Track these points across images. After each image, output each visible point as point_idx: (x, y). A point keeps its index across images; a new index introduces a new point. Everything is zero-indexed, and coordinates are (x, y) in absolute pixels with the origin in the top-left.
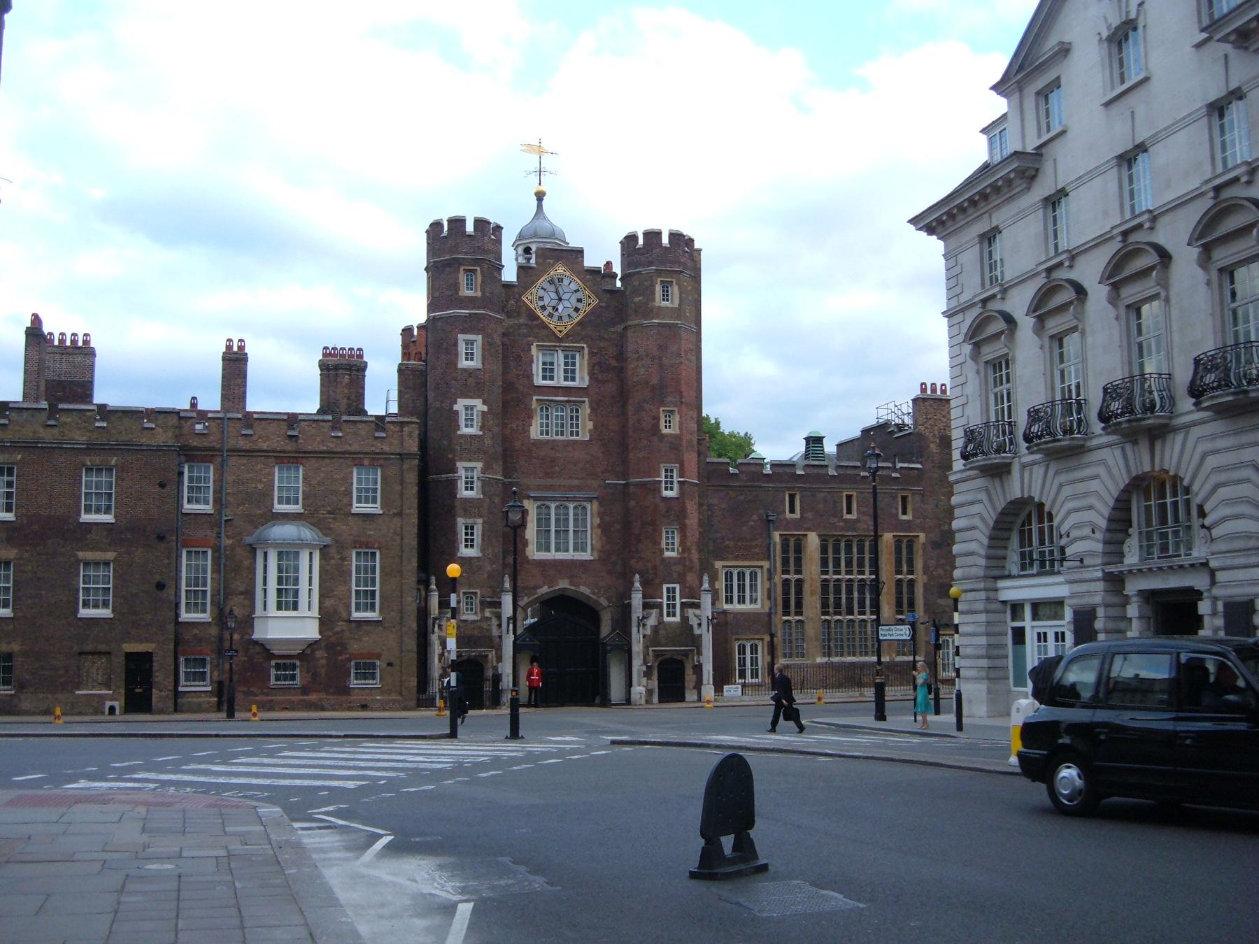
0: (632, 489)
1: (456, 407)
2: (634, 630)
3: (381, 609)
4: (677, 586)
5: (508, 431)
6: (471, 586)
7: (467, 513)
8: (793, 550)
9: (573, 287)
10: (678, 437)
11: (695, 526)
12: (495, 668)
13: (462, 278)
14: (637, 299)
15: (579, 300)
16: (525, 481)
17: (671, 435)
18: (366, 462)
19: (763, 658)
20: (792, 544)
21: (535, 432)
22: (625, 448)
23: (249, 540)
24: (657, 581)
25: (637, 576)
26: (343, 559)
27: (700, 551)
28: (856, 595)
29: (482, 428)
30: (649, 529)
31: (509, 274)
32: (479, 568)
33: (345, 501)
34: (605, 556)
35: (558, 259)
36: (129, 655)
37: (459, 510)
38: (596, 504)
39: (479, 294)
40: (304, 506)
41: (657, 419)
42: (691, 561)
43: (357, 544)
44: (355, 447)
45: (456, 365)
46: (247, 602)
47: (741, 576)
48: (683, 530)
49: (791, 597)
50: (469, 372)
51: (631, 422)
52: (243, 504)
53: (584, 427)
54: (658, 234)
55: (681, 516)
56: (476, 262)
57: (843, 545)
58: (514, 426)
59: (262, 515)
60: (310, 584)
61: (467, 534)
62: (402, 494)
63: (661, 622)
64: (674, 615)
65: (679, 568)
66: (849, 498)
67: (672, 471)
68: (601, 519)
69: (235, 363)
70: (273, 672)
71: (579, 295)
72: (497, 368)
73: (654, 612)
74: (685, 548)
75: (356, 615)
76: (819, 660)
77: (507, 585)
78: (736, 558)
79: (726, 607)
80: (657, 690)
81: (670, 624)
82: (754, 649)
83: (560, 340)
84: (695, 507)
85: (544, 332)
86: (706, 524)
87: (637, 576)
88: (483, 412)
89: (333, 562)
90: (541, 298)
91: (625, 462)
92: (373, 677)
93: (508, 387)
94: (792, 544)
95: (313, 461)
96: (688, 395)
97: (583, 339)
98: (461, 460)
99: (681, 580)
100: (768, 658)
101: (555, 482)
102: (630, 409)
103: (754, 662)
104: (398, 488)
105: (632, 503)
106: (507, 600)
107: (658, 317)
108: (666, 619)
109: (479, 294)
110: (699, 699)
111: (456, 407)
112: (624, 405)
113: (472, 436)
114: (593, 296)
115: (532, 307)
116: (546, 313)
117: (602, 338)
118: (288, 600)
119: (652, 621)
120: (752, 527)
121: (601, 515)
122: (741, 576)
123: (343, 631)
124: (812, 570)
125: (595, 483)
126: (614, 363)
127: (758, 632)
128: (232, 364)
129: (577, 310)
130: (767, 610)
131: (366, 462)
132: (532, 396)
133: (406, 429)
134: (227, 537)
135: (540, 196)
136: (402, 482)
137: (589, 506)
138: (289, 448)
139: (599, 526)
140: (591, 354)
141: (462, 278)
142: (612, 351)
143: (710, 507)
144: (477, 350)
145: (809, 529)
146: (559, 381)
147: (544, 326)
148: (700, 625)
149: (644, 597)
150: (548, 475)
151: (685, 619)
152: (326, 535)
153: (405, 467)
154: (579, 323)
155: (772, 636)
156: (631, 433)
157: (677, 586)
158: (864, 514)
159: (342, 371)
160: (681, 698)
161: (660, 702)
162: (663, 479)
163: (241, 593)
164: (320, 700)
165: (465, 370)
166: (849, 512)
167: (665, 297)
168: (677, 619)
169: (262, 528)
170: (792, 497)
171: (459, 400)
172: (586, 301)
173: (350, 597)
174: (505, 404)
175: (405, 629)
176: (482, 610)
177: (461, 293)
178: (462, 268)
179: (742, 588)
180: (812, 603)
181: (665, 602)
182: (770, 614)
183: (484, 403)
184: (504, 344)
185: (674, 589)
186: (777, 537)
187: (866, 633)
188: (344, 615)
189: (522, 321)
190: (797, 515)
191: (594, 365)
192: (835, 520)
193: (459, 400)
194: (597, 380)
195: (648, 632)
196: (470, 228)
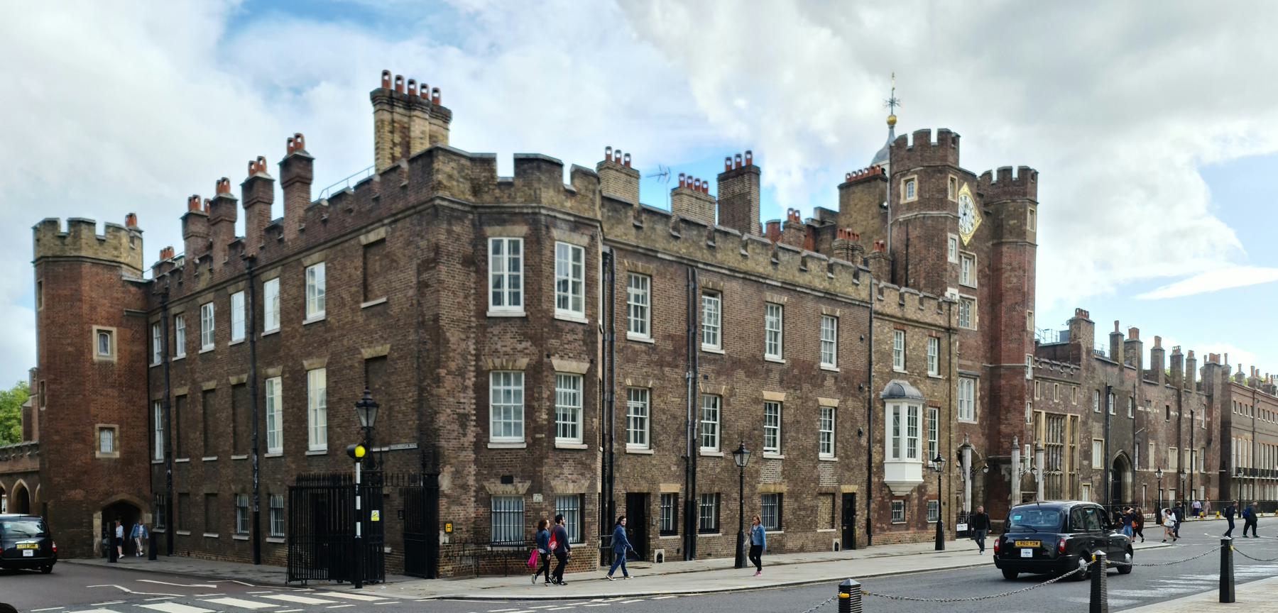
30: (1016, 401)
36: (845, 495)
125: (978, 365)
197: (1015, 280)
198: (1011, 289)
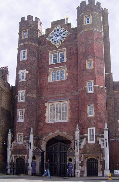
4: (94, 128)
6: (20, 132)
7: (21, 108)
9: (62, 31)
12: (27, 161)
21: (50, 80)
31: (44, 32)
32: (23, 125)
37: (18, 107)
38: (69, 102)
42: (100, 118)
61: (21, 114)
63: (87, 144)
64: (93, 141)
65: (94, 121)
67: (91, 83)
71: (64, 33)
73: (84, 140)
77: (32, 131)
81: (91, 144)
85: (53, 47)
90: (52, 37)
98: (19, 90)
99: (96, 126)
101: (56, 95)
106: (32, 136)
110: (103, 176)
116: (54, 41)
119: (83, 143)
121: (70, 105)
125: (68, 94)
126: (75, 52)
139: (70, 109)
142: (75, 48)
146: (59, 61)
147: (53, 45)
150: (53, 94)
151: (97, 142)
157: (94, 128)
160: (96, 175)
162: (88, 87)
168: (94, 142)
176: (24, 140)
183: (27, 70)
185: (93, 130)
191: (68, 55)
194: (70, 59)
195: (82, 147)
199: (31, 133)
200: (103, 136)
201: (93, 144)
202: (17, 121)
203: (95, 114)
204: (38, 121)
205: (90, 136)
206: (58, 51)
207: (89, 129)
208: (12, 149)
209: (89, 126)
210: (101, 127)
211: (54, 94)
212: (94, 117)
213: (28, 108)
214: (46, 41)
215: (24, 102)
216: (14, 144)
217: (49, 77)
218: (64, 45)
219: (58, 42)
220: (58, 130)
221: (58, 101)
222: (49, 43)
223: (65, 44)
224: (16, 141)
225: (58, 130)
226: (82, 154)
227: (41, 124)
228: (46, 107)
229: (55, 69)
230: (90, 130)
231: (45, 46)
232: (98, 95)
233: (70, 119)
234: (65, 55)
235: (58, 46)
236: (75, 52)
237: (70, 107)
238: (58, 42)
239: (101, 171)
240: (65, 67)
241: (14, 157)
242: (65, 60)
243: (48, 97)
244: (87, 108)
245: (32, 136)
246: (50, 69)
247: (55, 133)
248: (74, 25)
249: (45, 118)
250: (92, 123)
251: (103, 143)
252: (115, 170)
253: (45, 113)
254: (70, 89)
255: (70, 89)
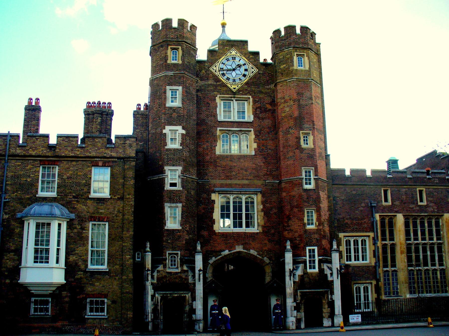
0: (283, 185)
1: (164, 131)
2: (287, 278)
3: (108, 263)
4: (316, 248)
5: (201, 150)
6: (174, 249)
8: (389, 225)
9: (242, 62)
10: (313, 150)
11: (326, 209)
12: (191, 305)
13: (170, 52)
14: (282, 67)
15: (246, 70)
16: (213, 182)
17: (308, 149)
18: (100, 164)
19: (372, 296)
20: (387, 221)
22: (278, 160)
23: (19, 215)
24: (302, 245)
25: (288, 243)
26: (83, 229)
27: (330, 226)
28: (429, 253)
29: (181, 144)
30: (296, 210)
32: (180, 237)
33: (86, 189)
34: (266, 229)
35: (232, 46)
38: (260, 196)
39: (180, 62)
40: (57, 193)
41: (299, 138)
42: (324, 231)
43: (92, 218)
44: (93, 154)
45: (165, 105)
46: (16, 257)
47: (356, 242)
48: (318, 211)
49: (387, 255)
50: (173, 109)
51: (281, 142)
52: (17, 191)
53: (251, 147)
54: (294, 27)
55: (317, 201)
56: (178, 43)
57: (418, 221)
58: (205, 146)
59: (29, 199)
60: (59, 245)
62: (124, 185)
63: (305, 273)
64: (314, 268)
65: (316, 236)
66: (421, 192)
67: (310, 172)
68: (264, 206)
69: (33, 112)
70: (33, 306)
71: (246, 67)
72: (193, 108)
73: (301, 266)
74: (320, 223)
75: (91, 267)
76: (408, 296)
78: (352, 231)
79: (347, 263)
80: (303, 319)
81: (312, 273)
82: (366, 290)
83: (234, 93)
84: (326, 196)
85: (225, 89)
86: (332, 209)
87: (288, 243)
88: (182, 134)
89: (75, 231)
91: (278, 168)
92: (102, 310)
93: (200, 123)
94: (387, 221)
95: (65, 163)
96: (318, 124)
97: (249, 93)
98: (168, 165)
100: (375, 296)
102: (281, 134)
103: (366, 297)
104: (121, 181)
105: (284, 194)
106: (199, 259)
107: (296, 75)
108: (309, 270)
109: (180, 62)
110: (333, 326)
111: (164, 131)
112: (277, 133)
113: (174, 150)
114: (254, 67)
115: (217, 74)
116: (225, 77)
117: (261, 92)
118: (41, 256)
119: (299, 272)
120: (361, 211)
121: (263, 203)
122: (356, 242)
123: (81, 278)
124: (400, 237)
125: (259, 183)
126: (269, 107)
127: (367, 279)
128: (30, 112)
129: (244, 76)
130: (373, 264)
131: (100, 164)
132: (216, 127)
133: (128, 142)
134: (6, 213)
135: (223, 25)
136: (124, 178)
137: (255, 197)
138: (49, 154)
139: (262, 210)
140: (255, 102)
141: (170, 52)
142: (268, 100)
143: (334, 197)
144: (179, 95)
145: (397, 212)
146: (234, 117)
147: (224, 85)
148: (332, 274)
149: (293, 256)
150: (228, 177)
151: (321, 270)
152: (71, 212)
153: (126, 167)
154: (247, 84)
155: (378, 281)
156: (281, 149)
157: (316, 248)
158: (431, 202)
159: (99, 116)
160: (320, 325)
161: (307, 326)
163: (12, 251)
164: (63, 326)
165: (171, 108)
166: (421, 201)
167: (300, 64)
168: (317, 270)
169: (28, 208)
170: (385, 192)
171: (166, 127)
172: (250, 70)
173: (87, 254)
174: (199, 133)
175: (124, 277)
176: (182, 265)
177: (169, 62)
178: (169, 47)
179: (356, 250)
180: (401, 259)
181: (308, 258)
182: (375, 267)
183: (183, 128)
184: (197, 95)
185: (314, 250)
186: (377, 217)
187: (437, 278)
188: (83, 267)
189: (210, 82)
190: (390, 203)
191: (256, 109)
192: (413, 206)
193: (166, 127)
194: (259, 118)
195: (297, 280)
196: (175, 24)
197: (287, 109)
198: (285, 117)
199: (196, 252)
200: (330, 262)
201: (315, 273)
202: (166, 228)
203: (317, 224)
204: (200, 228)
205: (310, 261)
206: (234, 97)
207: (308, 248)
208: (155, 281)
209: (307, 244)
210: (325, 246)
211: (231, 179)
212: (317, 230)
213: (186, 203)
214: (209, 74)
215: (180, 191)
216: (158, 271)
217: (218, 144)
218: (246, 90)
219: (234, 81)
220: (241, 247)
221: (239, 193)
222: (217, 79)
223: (249, 89)
224: (165, 266)
225: (241, 247)
226: (299, 291)
227: (205, 233)
228: (214, 201)
229: (229, 130)
230: (310, 250)
231: (206, 83)
232: (320, 194)
233: (263, 227)
234: (248, 109)
235: (234, 88)
236: (269, 107)
237: (261, 207)
238: (234, 81)
239: (329, 317)
240: (251, 131)
241: (159, 298)
242: (249, 117)
243: (218, 182)
244: (303, 214)
245: (199, 259)
246: (220, 130)
247: (235, 251)
248: (266, 55)
249: (213, 222)
250: (314, 240)
251: (331, 272)
252: (350, 316)
253: (213, 212)
254: (261, 174)
255: (261, 174)
